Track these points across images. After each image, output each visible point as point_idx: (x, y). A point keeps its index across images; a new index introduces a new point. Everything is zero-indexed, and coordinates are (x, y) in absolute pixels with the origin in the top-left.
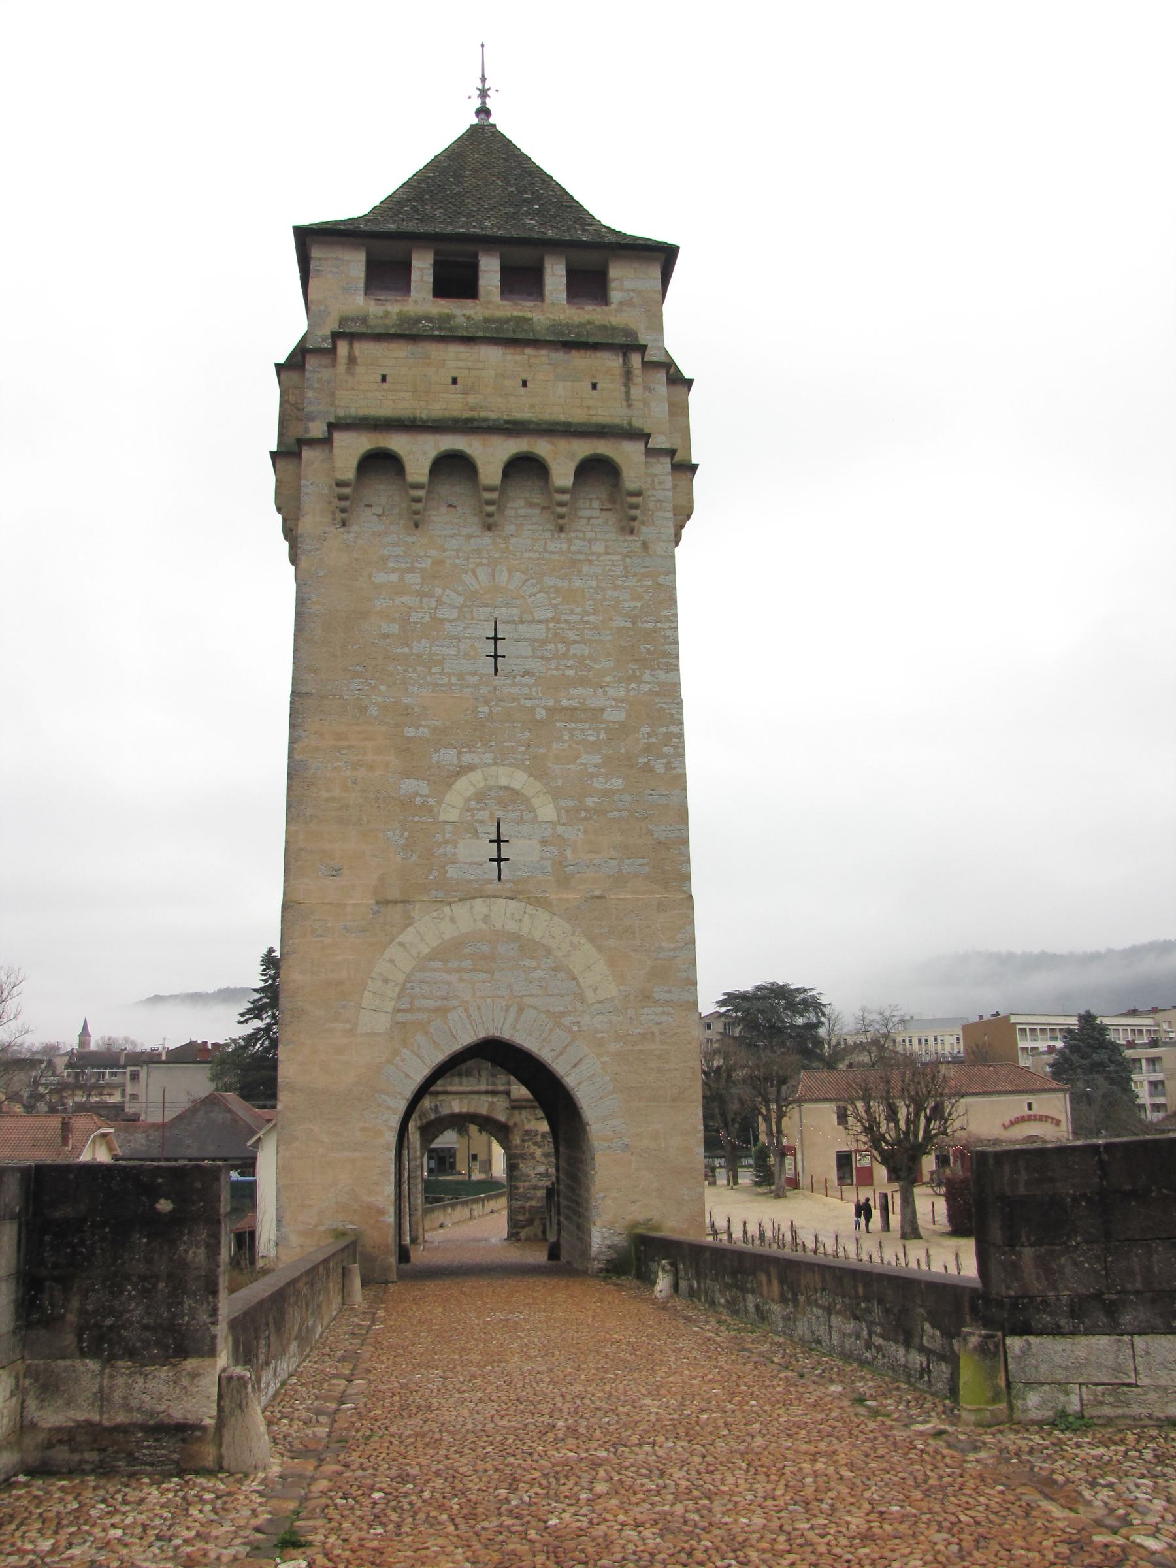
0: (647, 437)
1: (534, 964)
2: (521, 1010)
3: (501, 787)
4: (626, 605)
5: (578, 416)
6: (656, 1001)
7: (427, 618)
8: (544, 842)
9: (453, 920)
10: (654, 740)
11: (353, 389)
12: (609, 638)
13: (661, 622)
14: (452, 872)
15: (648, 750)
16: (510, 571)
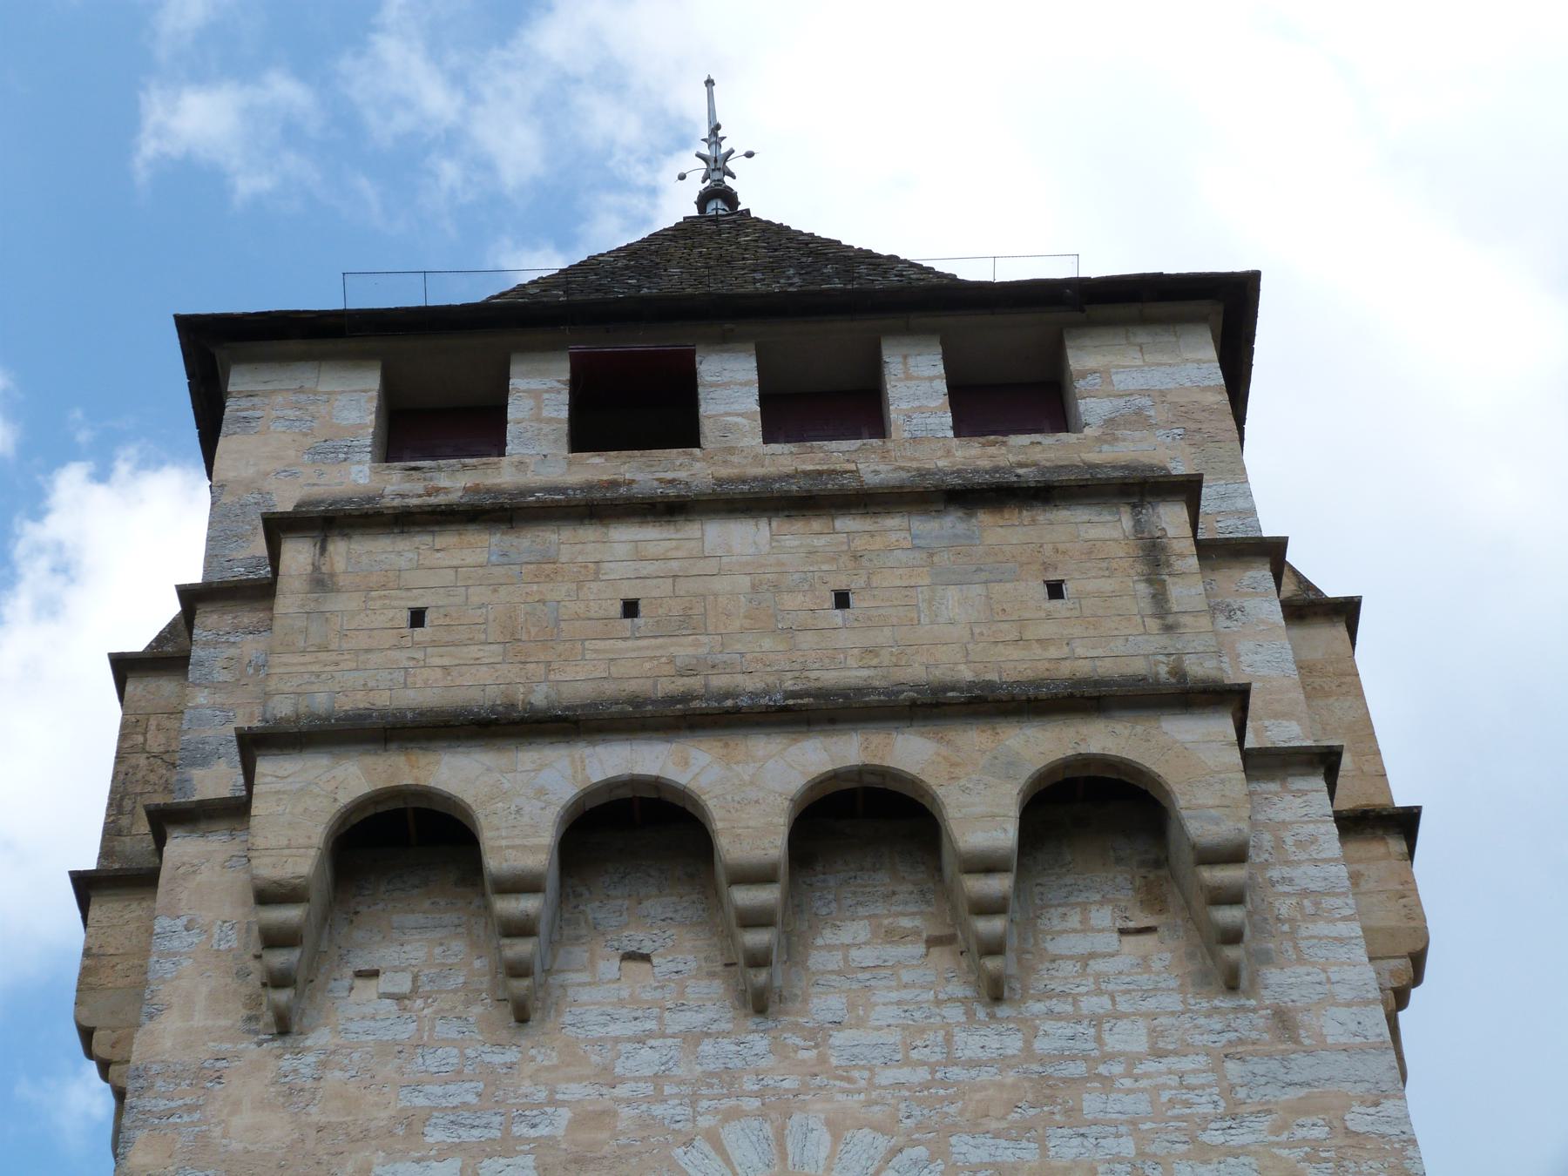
0: (1233, 699)
5: (1014, 663)
16: (836, 1127)
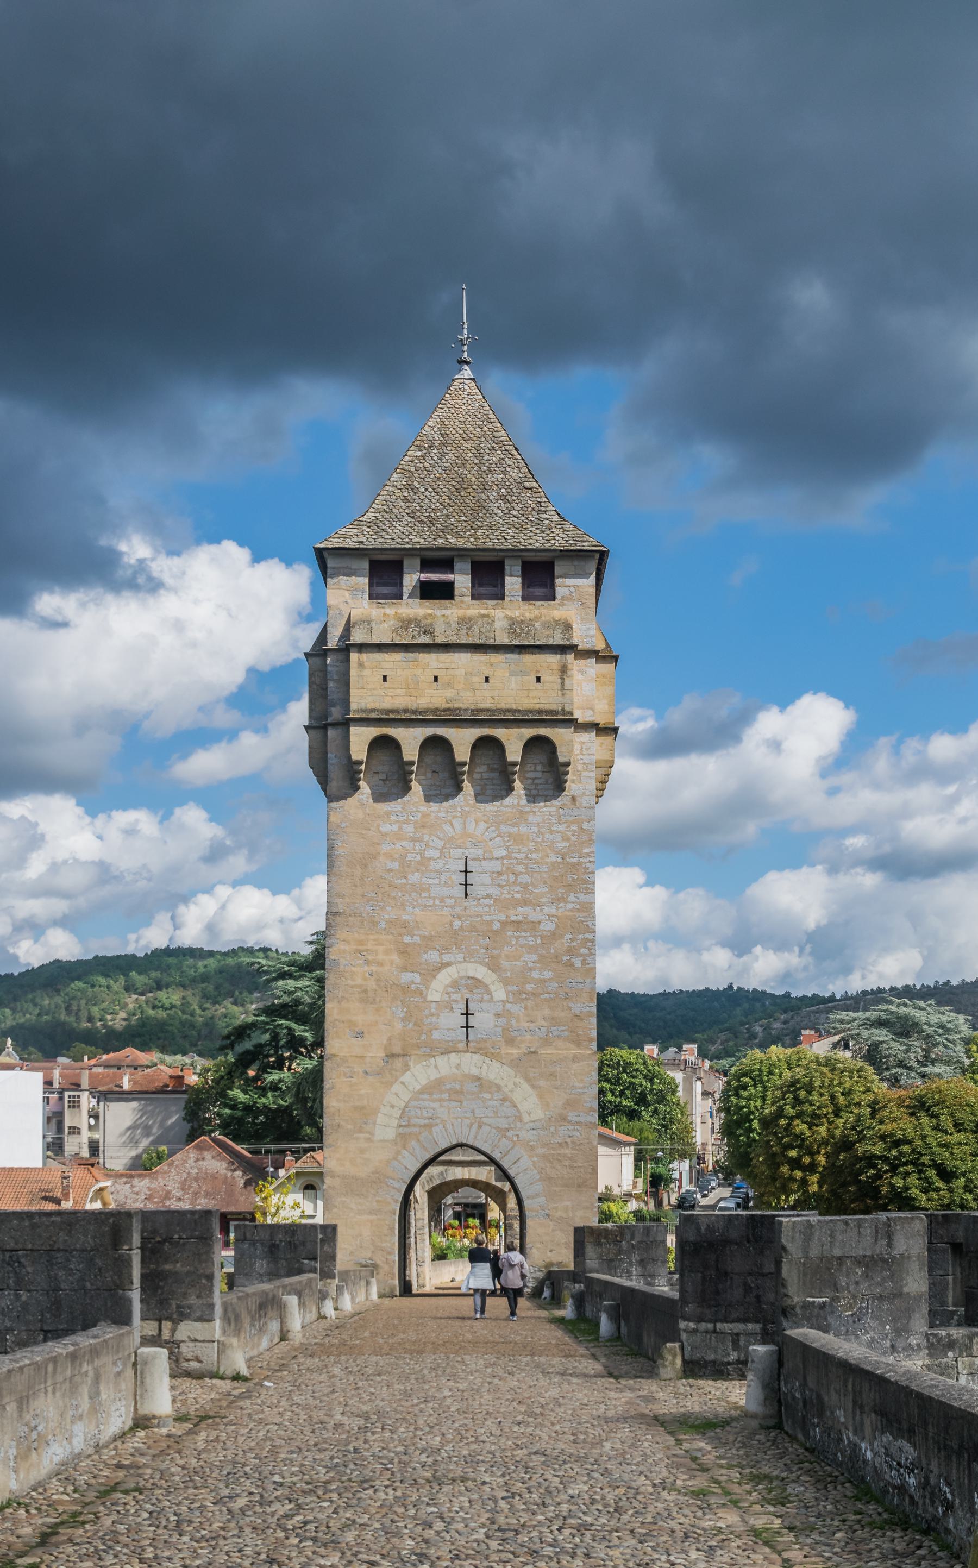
1: (489, 1096)
2: (480, 1127)
3: (469, 978)
4: (559, 845)
6: (570, 1122)
7: (418, 858)
8: (498, 1015)
9: (436, 1067)
10: (574, 944)
11: (363, 688)
12: (546, 870)
13: (583, 857)
14: (436, 1035)
15: (570, 951)
16: (476, 822)
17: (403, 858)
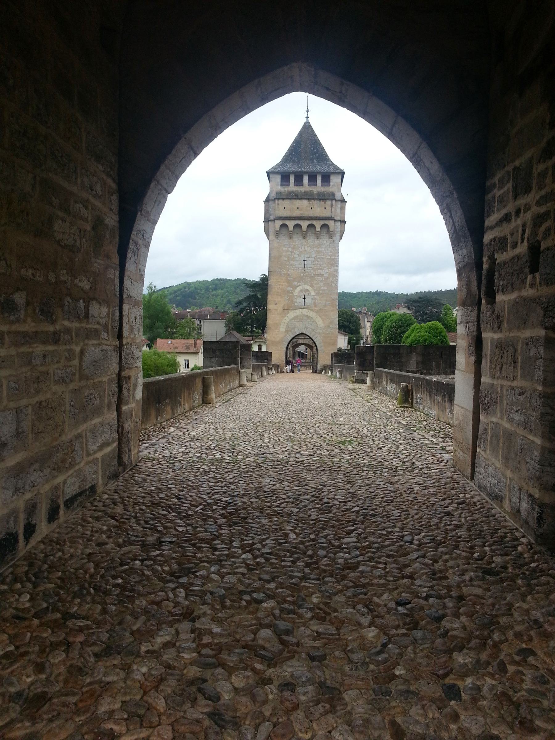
15: (332, 282)
17: (288, 257)
